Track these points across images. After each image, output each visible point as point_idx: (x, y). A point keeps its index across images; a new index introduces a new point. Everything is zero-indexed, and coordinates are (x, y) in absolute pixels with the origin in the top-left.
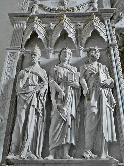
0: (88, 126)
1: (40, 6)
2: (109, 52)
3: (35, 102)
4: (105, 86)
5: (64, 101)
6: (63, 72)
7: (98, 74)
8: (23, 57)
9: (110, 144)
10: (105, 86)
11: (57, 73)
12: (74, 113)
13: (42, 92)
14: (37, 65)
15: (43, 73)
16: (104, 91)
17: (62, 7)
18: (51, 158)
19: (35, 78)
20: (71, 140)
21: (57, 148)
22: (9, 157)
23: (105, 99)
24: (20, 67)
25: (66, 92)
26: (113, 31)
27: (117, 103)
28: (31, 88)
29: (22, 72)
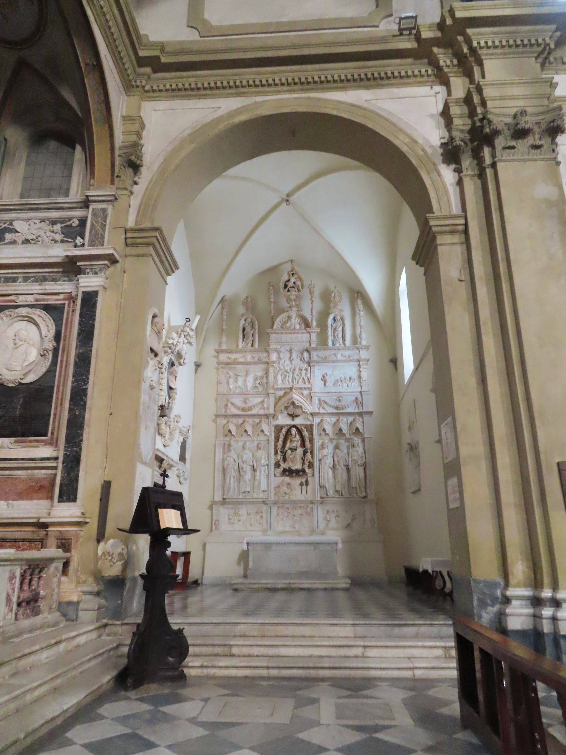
0: (256, 484)
1: (232, 404)
2: (268, 443)
3: (233, 474)
4: (264, 466)
5: (245, 472)
6: (245, 457)
7: (261, 459)
8: (224, 444)
9: (264, 491)
10: (264, 466)
11: (242, 457)
12: (250, 478)
13: (236, 468)
14: (233, 452)
15: (235, 457)
16: (263, 468)
17: (245, 406)
18: (240, 497)
19: (232, 460)
20: (248, 489)
21: (243, 493)
22: (224, 497)
23: (263, 472)
24: (224, 453)
25: (246, 468)
26: (273, 428)
27: (268, 473)
28: (231, 466)
29: (225, 456)
